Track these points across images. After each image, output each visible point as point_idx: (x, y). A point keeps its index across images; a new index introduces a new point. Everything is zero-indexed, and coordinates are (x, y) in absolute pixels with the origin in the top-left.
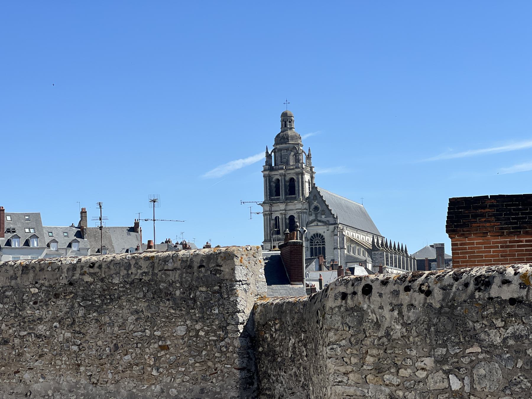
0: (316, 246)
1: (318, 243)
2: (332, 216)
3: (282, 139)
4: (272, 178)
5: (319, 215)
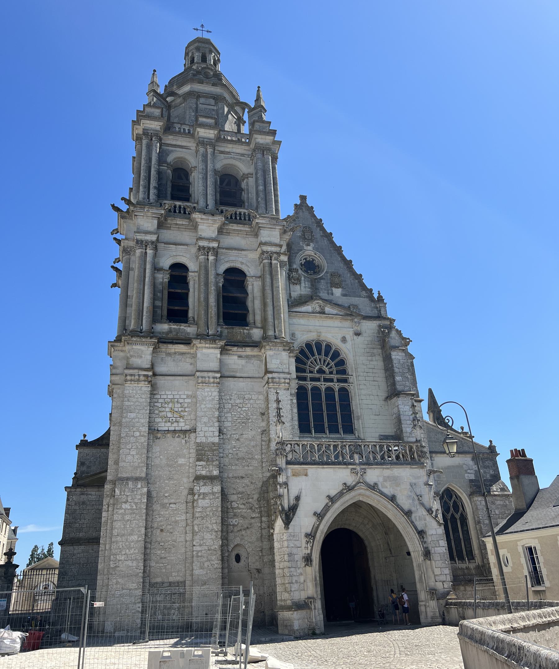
0: (318, 383)
1: (324, 372)
2: (364, 293)
4: (168, 153)
5: (322, 285)
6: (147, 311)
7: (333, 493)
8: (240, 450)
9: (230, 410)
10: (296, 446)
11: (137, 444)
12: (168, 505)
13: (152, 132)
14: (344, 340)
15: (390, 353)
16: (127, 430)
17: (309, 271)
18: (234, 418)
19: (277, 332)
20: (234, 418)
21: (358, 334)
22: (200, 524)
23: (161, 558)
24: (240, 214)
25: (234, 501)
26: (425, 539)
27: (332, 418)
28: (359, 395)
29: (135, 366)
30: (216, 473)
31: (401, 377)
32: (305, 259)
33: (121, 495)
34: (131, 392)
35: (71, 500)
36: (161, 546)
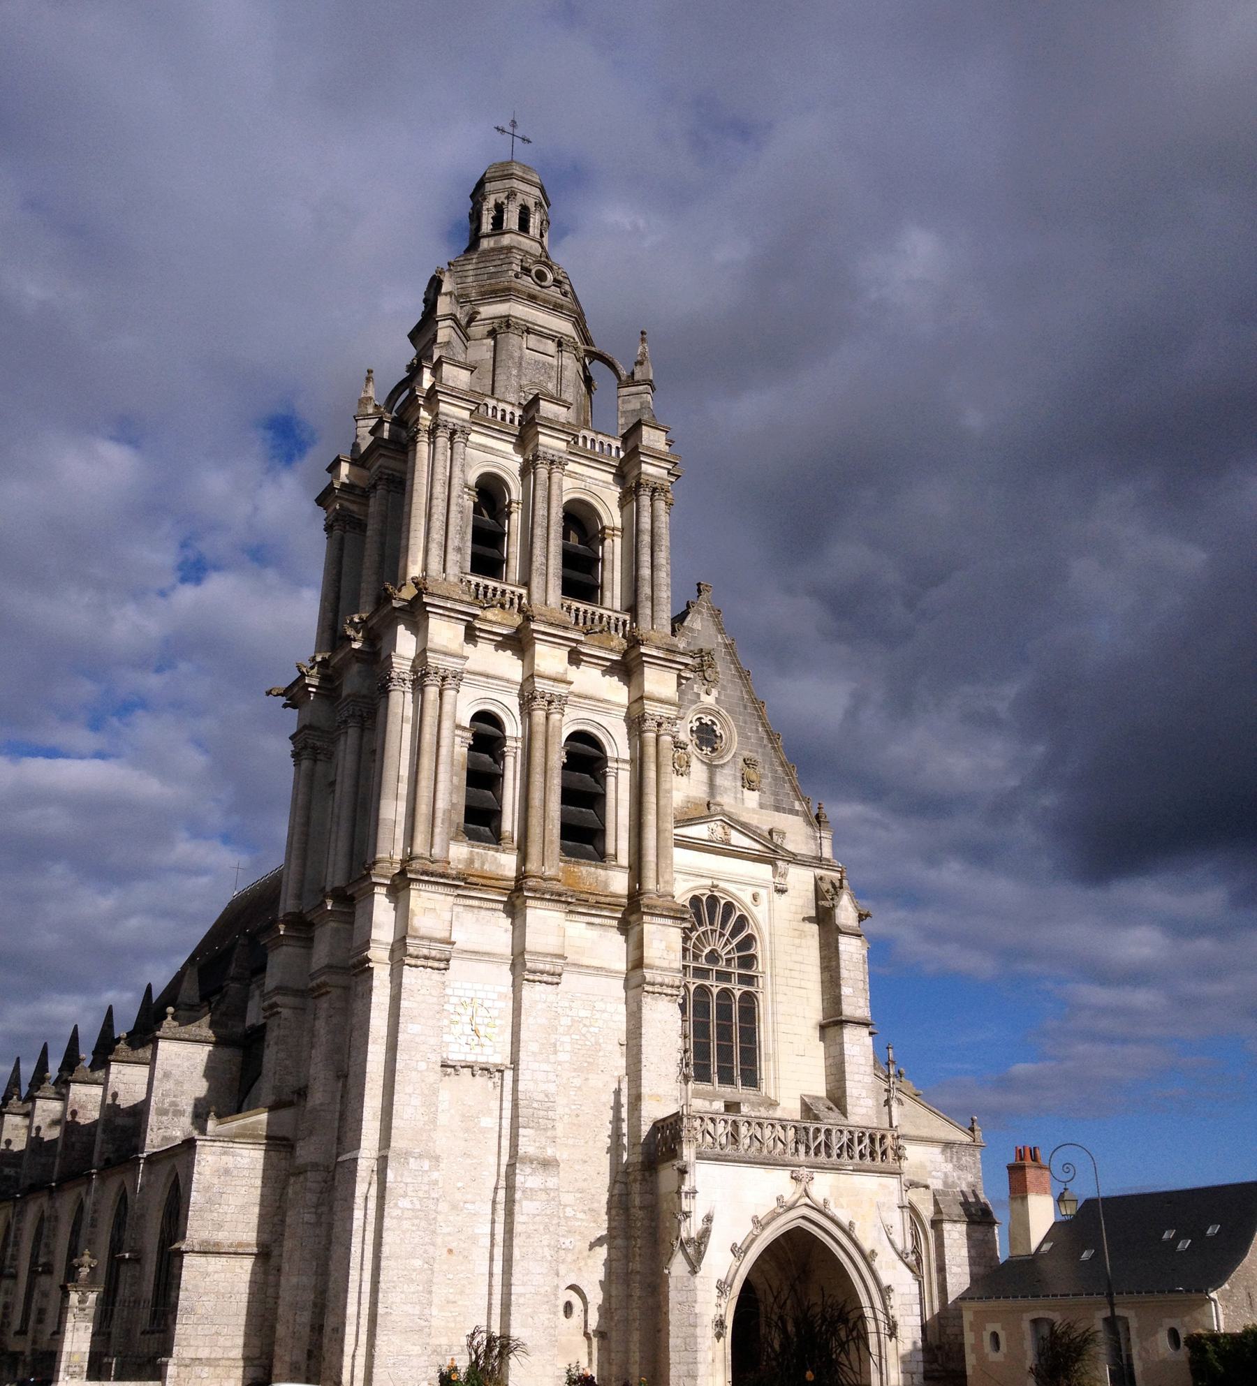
2: (797, 806)
3: (526, 271)
6: (443, 819)
7: (762, 1214)
8: (583, 1108)
9: (569, 1030)
10: (709, 1122)
11: (423, 1084)
12: (461, 1204)
13: (455, 421)
14: (755, 897)
15: (837, 940)
16: (407, 1057)
17: (704, 748)
18: (575, 1046)
19: (662, 884)
20: (575, 1046)
21: (781, 891)
22: (524, 1246)
23: (448, 1302)
24: (601, 616)
25: (569, 1205)
26: (892, 1302)
27: (725, 1054)
28: (773, 1013)
29: (422, 932)
30: (550, 1152)
31: (851, 990)
32: (699, 719)
33: (395, 1182)
34: (413, 981)
35: (203, 1163)
36: (449, 1279)
